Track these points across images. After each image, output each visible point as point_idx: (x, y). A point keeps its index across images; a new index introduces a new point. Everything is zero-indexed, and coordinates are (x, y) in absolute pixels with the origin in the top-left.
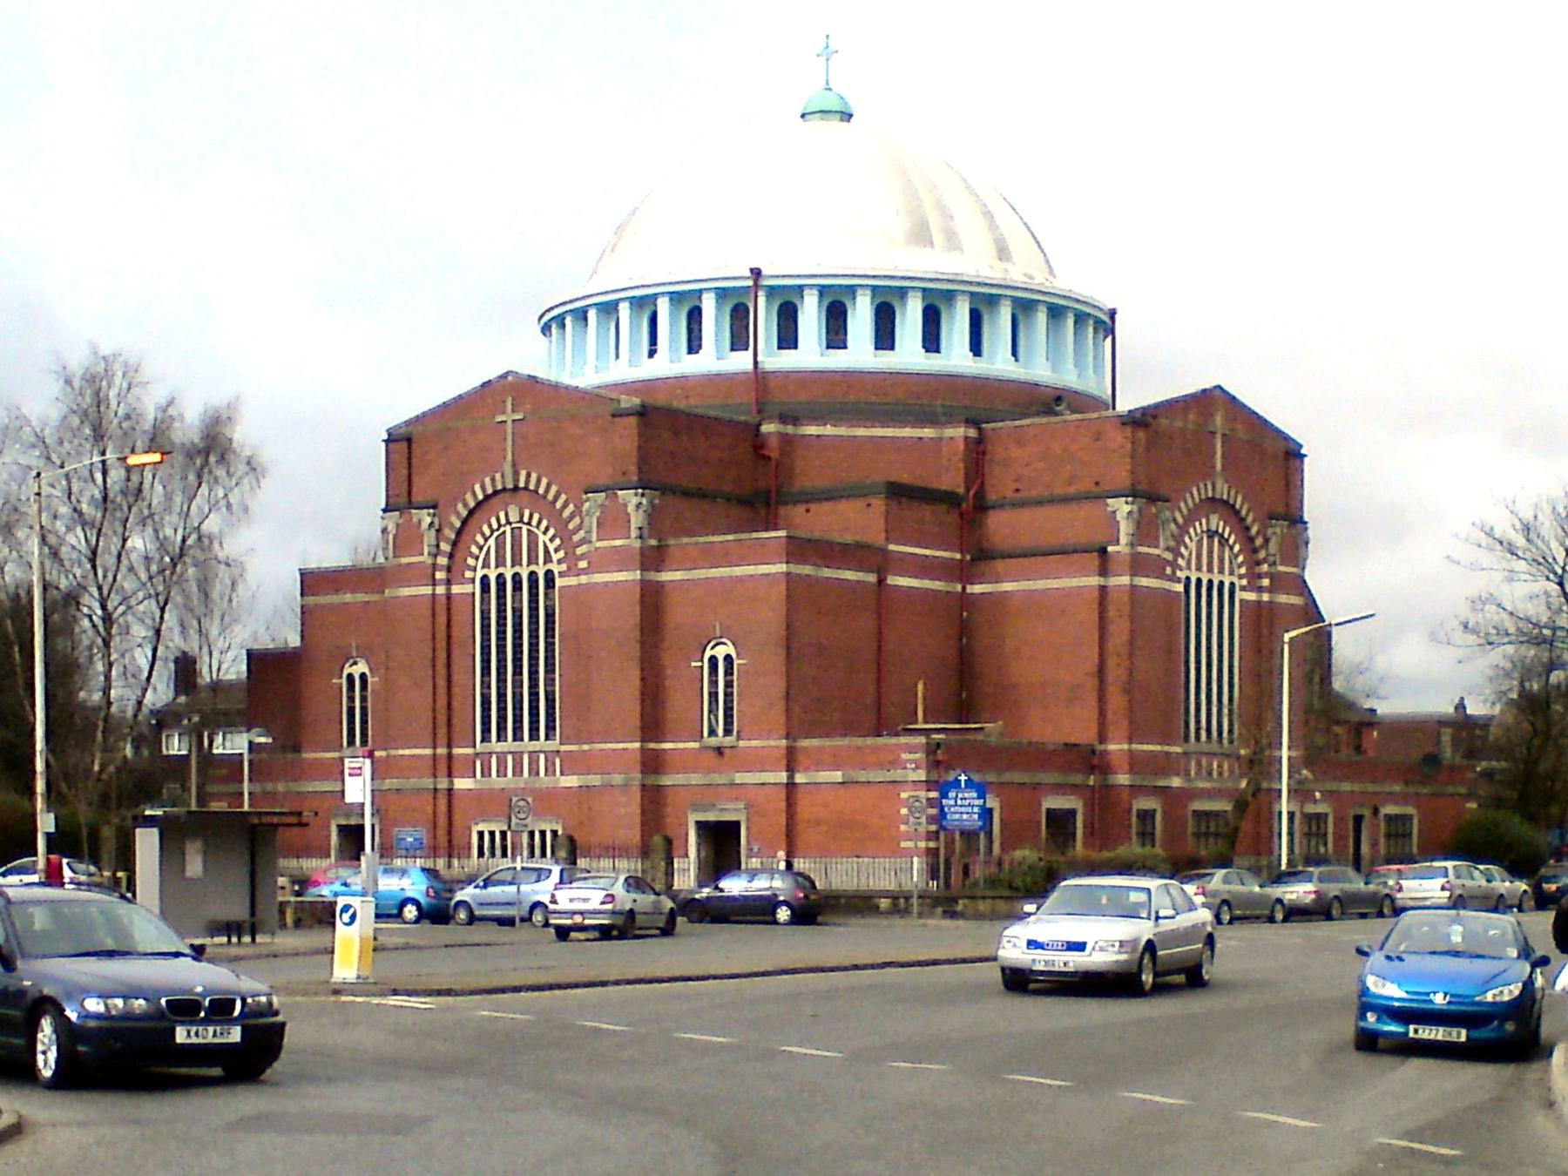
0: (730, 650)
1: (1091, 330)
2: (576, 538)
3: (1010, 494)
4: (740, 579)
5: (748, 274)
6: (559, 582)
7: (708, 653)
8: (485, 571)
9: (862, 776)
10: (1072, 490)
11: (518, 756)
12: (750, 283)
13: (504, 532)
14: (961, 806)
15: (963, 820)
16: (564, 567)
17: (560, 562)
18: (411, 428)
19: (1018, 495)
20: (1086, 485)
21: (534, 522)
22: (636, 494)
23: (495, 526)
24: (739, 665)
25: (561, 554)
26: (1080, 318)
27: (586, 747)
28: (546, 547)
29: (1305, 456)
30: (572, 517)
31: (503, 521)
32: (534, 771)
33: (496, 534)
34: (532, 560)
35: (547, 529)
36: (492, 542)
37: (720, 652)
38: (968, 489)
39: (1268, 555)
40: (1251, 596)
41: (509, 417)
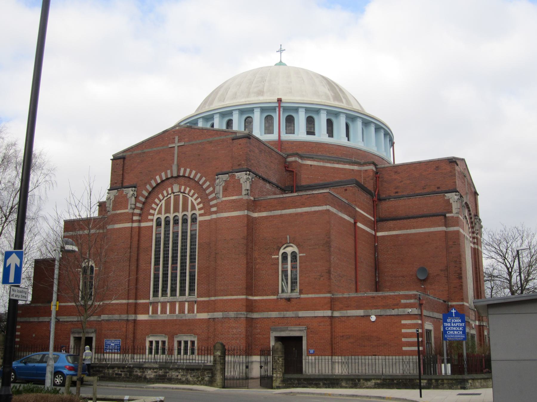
0: (295, 249)
3: (393, 194)
4: (301, 214)
5: (276, 101)
6: (199, 219)
7: (282, 251)
8: (159, 216)
11: (173, 304)
12: (277, 105)
13: (170, 197)
14: (453, 327)
15: (455, 335)
17: (200, 209)
18: (124, 154)
19: (397, 194)
21: (187, 192)
22: (246, 174)
23: (165, 194)
24: (300, 256)
25: (201, 205)
27: (213, 298)
28: (192, 202)
30: (208, 187)
31: (170, 192)
32: (182, 311)
33: (165, 198)
34: (185, 209)
35: (194, 194)
36: (163, 202)
37: (289, 250)
41: (176, 145)
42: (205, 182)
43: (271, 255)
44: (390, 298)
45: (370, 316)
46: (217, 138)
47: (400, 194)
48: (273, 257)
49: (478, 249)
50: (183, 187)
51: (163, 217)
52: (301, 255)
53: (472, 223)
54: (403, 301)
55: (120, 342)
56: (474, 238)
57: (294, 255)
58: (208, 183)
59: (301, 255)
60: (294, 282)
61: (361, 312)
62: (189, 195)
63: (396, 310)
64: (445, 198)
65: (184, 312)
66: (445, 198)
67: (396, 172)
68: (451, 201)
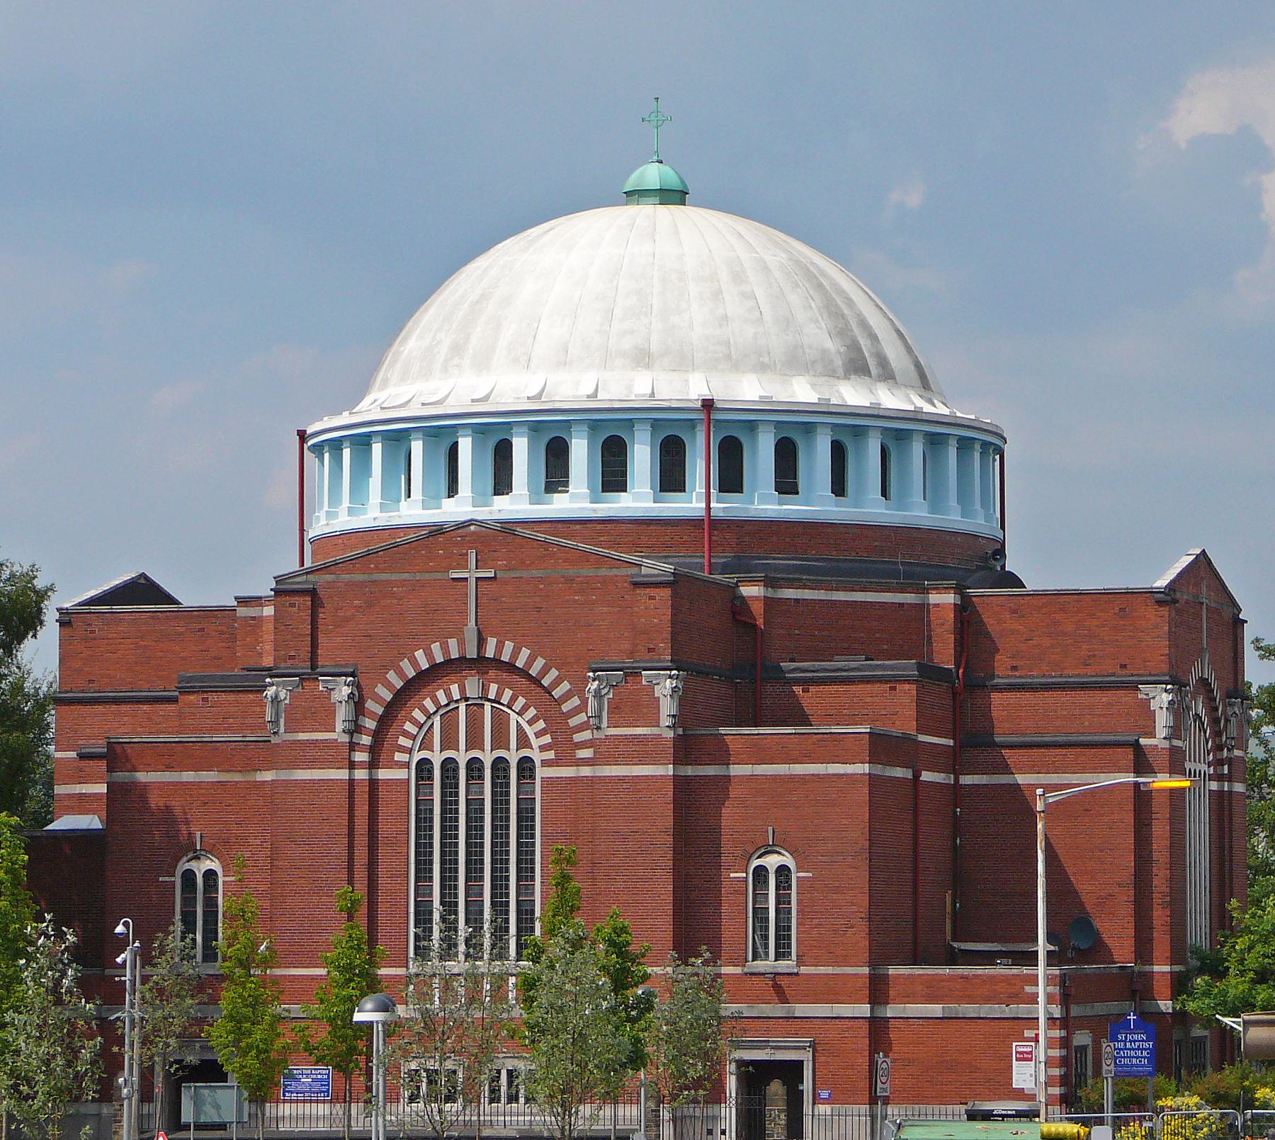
0: (788, 860)
1: (977, 456)
2: (573, 722)
4: (803, 779)
5: (699, 404)
6: (540, 773)
8: (425, 754)
9: (970, 1010)
14: (1130, 1049)
15: (1132, 1065)
16: (551, 755)
17: (543, 748)
21: (505, 700)
22: (670, 677)
25: (547, 739)
26: (965, 445)
30: (567, 696)
31: (456, 696)
34: (500, 739)
38: (958, 666)
40: (1214, 786)
41: (472, 573)
42: (557, 682)
44: (1002, 981)
46: (587, 571)
48: (732, 875)
49: (1230, 792)
50: (493, 688)
51: (437, 758)
53: (1215, 721)
55: (329, 1075)
57: (782, 870)
58: (565, 686)
68: (1154, 705)
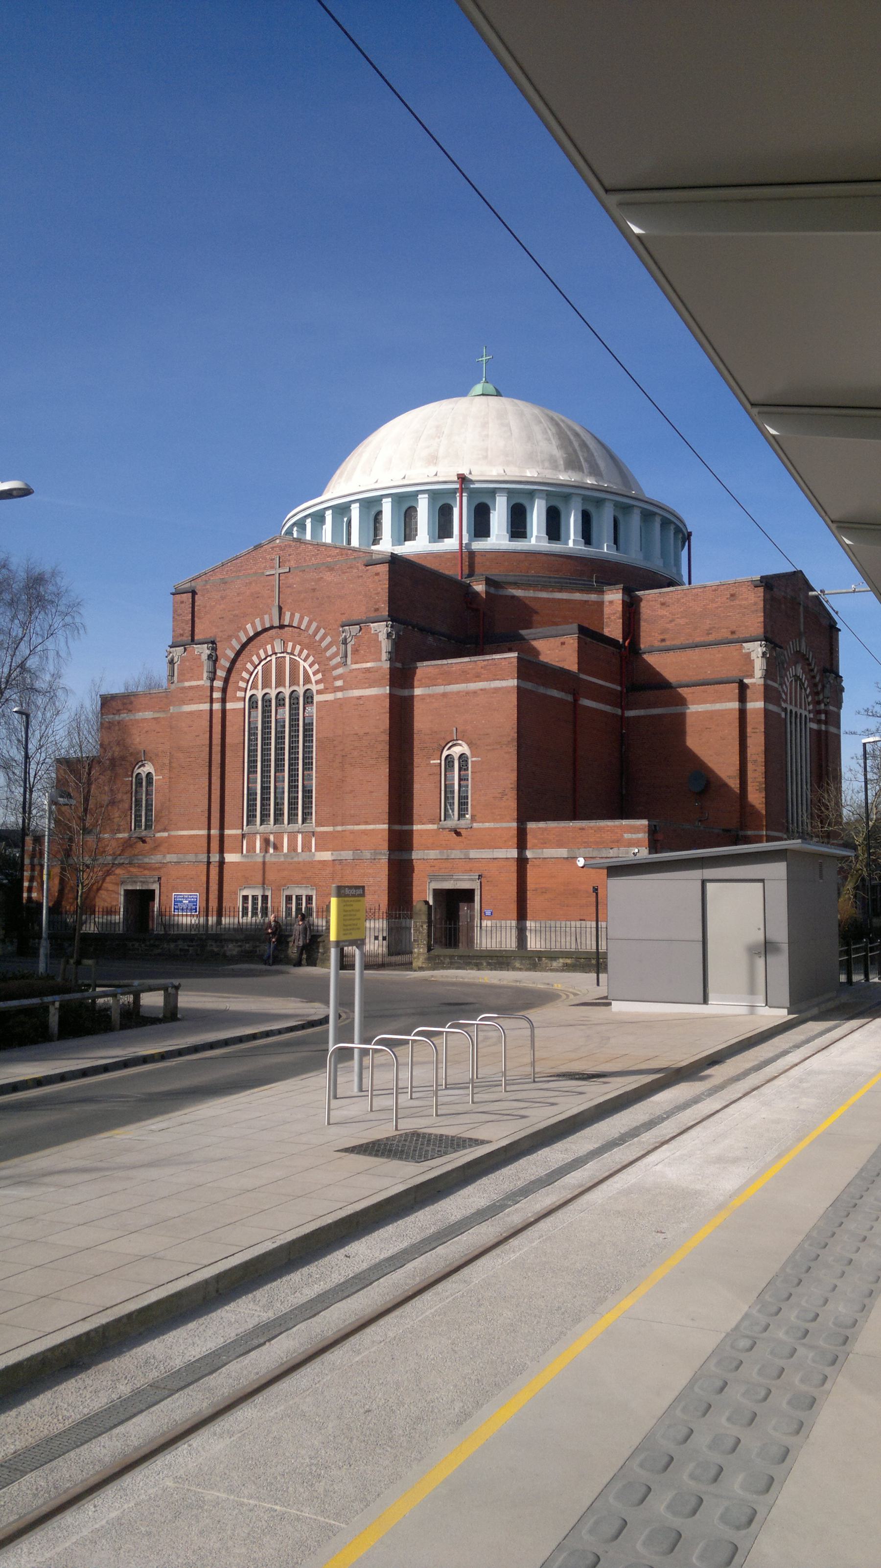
3: (657, 644)
5: (456, 479)
6: (317, 698)
7: (445, 753)
8: (254, 692)
10: (711, 638)
12: (457, 486)
13: (271, 660)
16: (321, 686)
17: (317, 682)
18: (193, 584)
19: (663, 644)
20: (725, 634)
21: (296, 652)
23: (263, 656)
24: (472, 762)
25: (319, 676)
27: (339, 828)
29: (840, 630)
31: (270, 653)
34: (294, 681)
37: (456, 751)
38: (624, 639)
39: (824, 697)
40: (814, 726)
42: (323, 638)
43: (429, 758)
44: (608, 831)
45: (577, 858)
47: (668, 643)
48: (432, 762)
49: (827, 732)
50: (290, 644)
51: (259, 694)
52: (474, 759)
54: (627, 836)
56: (819, 712)
59: (474, 759)
60: (463, 804)
61: (563, 852)
62: (299, 657)
63: (615, 850)
64: (744, 651)
65: (295, 850)
66: (744, 651)
67: (663, 604)
68: (753, 656)
